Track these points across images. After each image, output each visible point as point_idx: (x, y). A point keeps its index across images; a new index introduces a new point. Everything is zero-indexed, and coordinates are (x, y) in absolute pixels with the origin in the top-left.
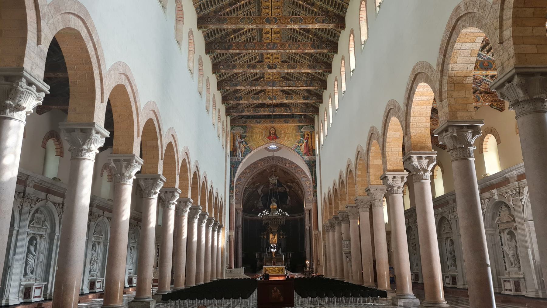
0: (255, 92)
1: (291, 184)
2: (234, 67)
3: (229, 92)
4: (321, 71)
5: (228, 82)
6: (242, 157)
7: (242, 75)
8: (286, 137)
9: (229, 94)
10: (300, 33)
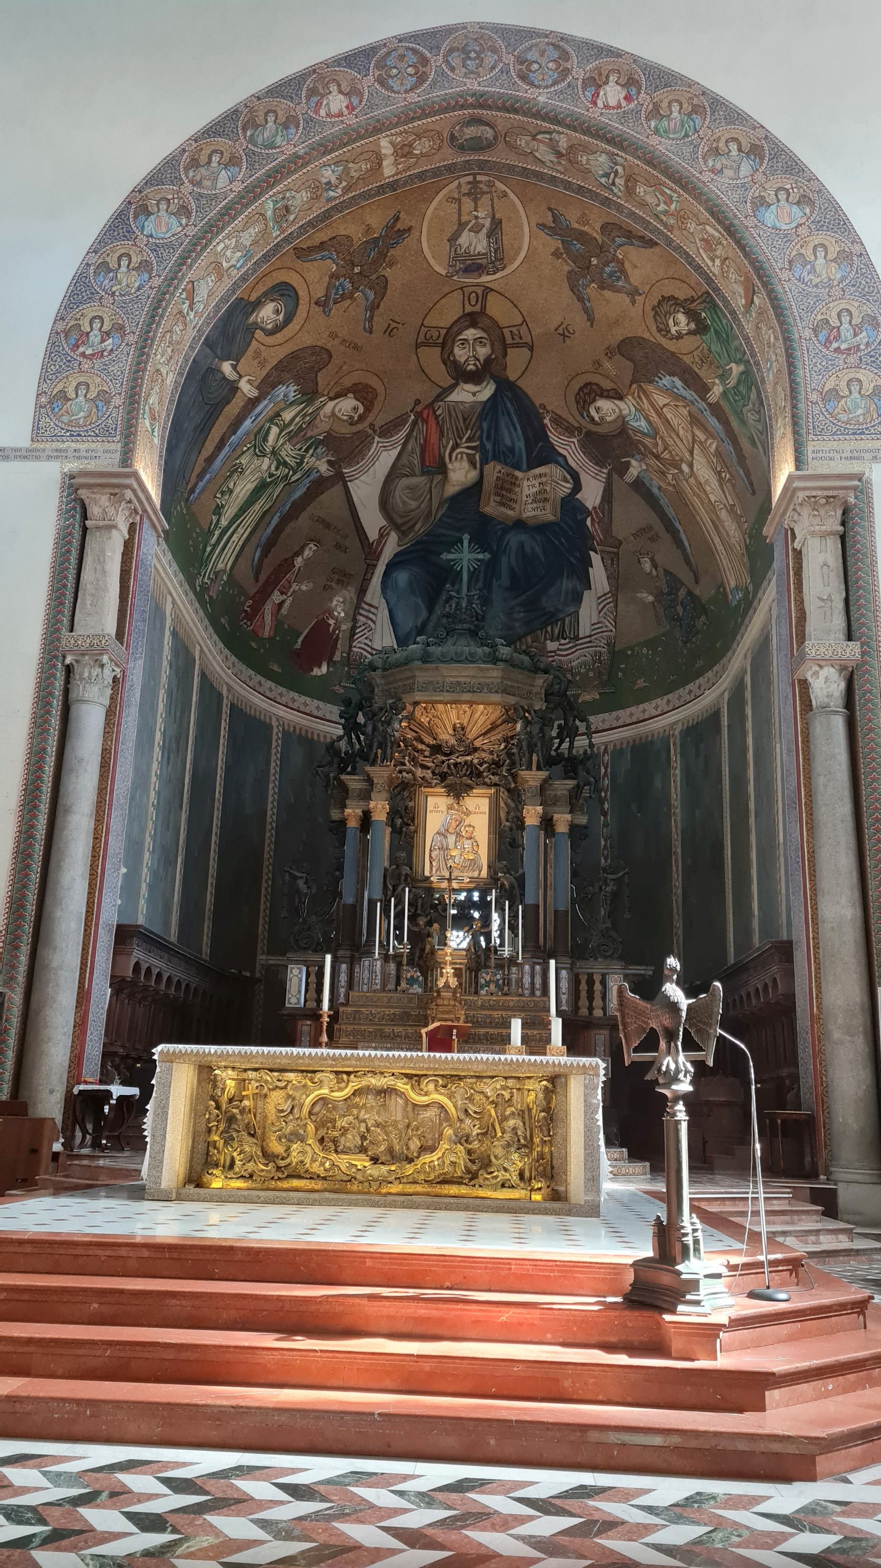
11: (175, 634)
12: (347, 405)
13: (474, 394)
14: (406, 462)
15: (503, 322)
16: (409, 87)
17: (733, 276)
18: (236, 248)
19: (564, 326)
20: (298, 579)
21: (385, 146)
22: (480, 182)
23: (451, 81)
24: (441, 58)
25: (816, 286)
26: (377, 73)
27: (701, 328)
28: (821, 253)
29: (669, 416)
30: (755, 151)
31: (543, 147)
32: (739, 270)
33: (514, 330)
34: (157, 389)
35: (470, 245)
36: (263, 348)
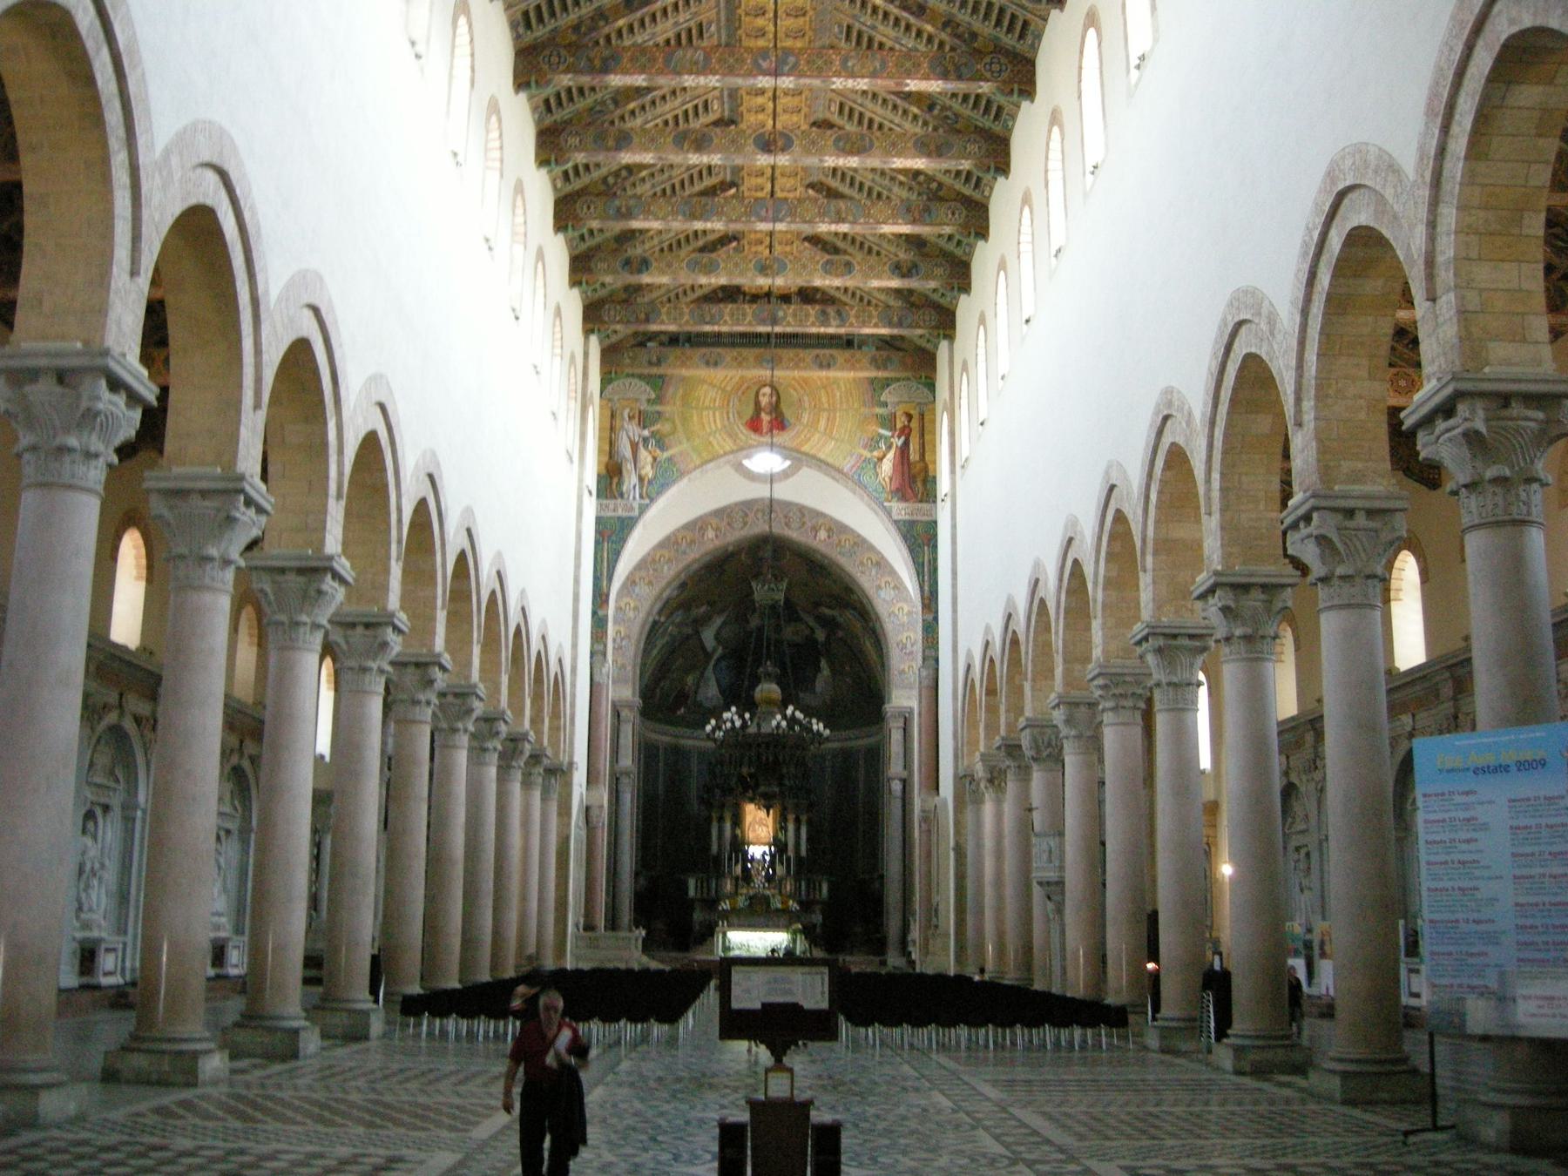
0: (701, 243)
1: (835, 613)
2: (623, 141)
3: (598, 239)
4: (966, 165)
5: (594, 199)
6: (641, 497)
7: (653, 175)
8: (823, 423)
9: (598, 247)
10: (886, 15)
30: (878, 564)
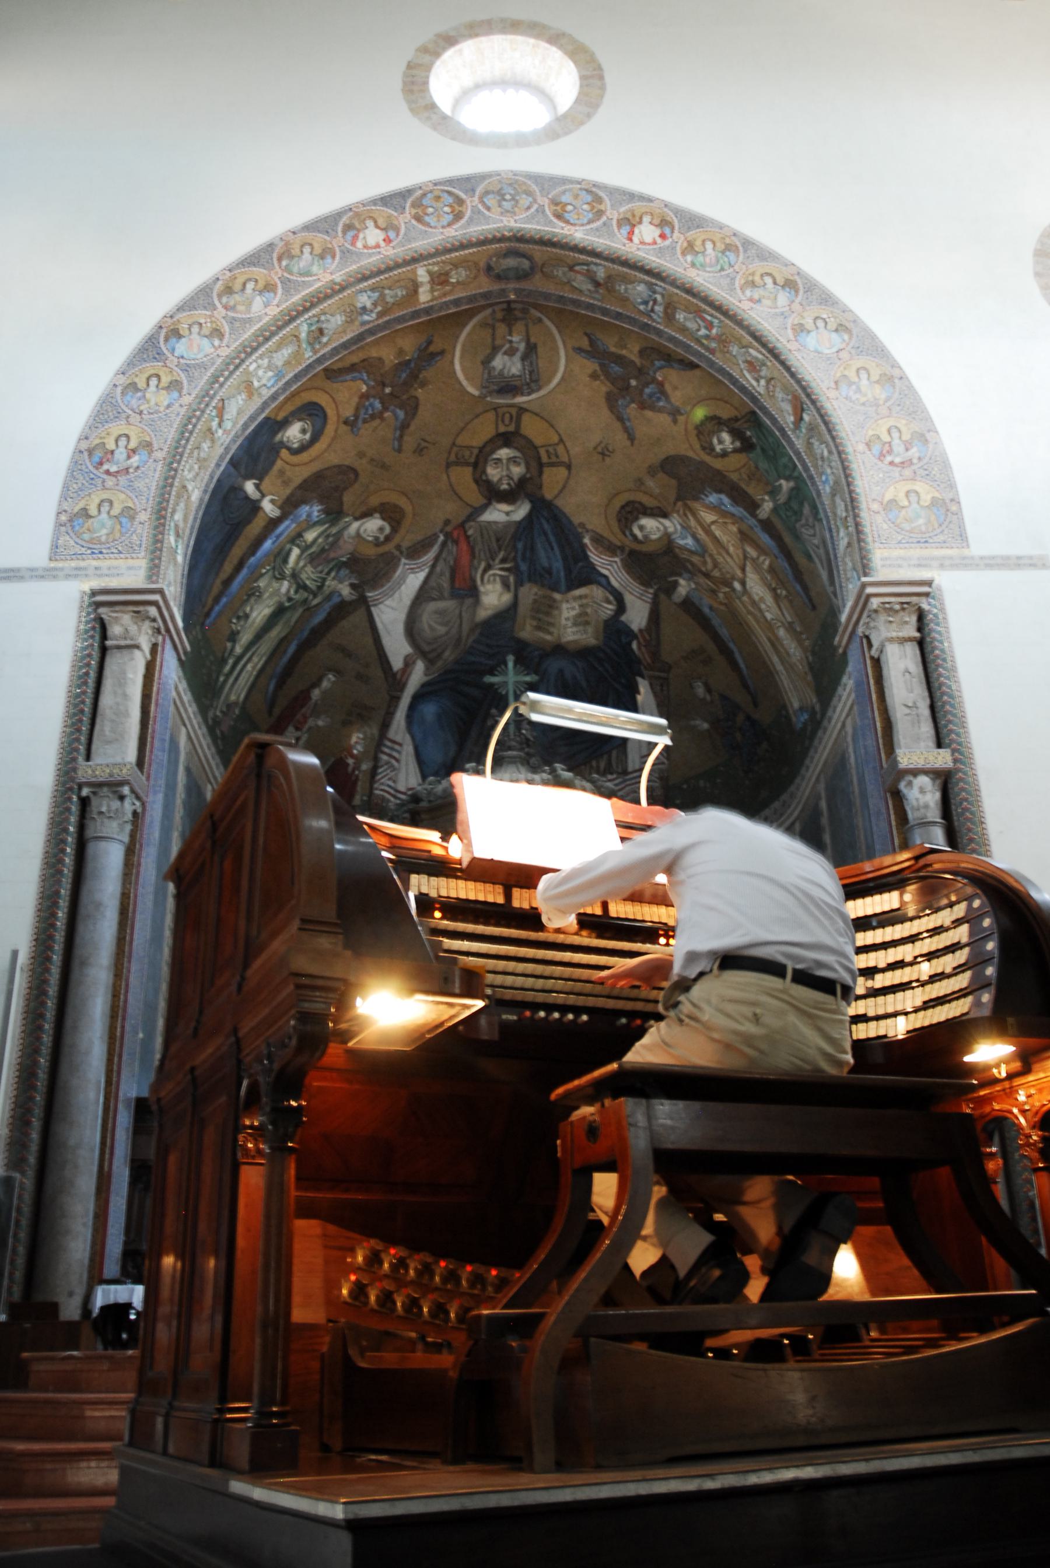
11: (188, 770)
12: (373, 526)
13: (507, 514)
14: (434, 584)
15: (538, 441)
16: (445, 223)
17: (780, 395)
18: (269, 368)
19: (603, 445)
20: (316, 713)
21: (422, 274)
22: (515, 309)
23: (487, 219)
24: (476, 199)
25: (863, 404)
26: (414, 211)
27: (747, 446)
28: (863, 375)
29: (718, 533)
30: (790, 285)
31: (580, 277)
32: (786, 389)
33: (551, 449)
34: (182, 505)
35: (504, 368)
36: (287, 467)
